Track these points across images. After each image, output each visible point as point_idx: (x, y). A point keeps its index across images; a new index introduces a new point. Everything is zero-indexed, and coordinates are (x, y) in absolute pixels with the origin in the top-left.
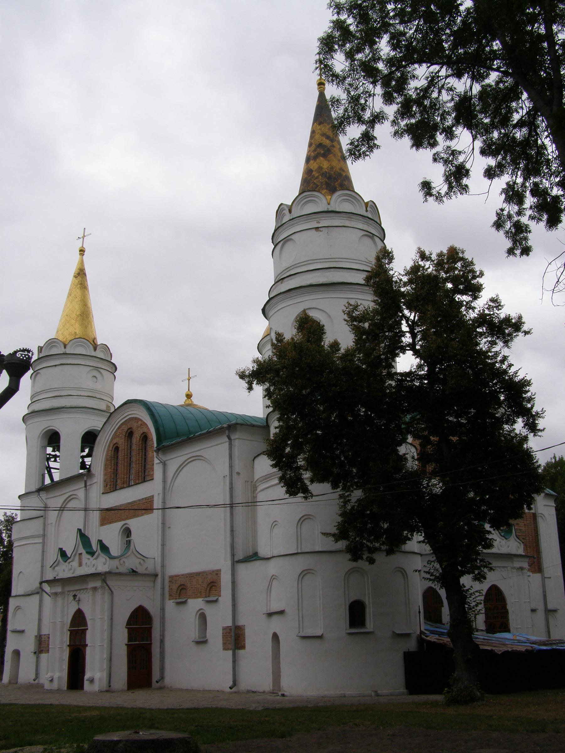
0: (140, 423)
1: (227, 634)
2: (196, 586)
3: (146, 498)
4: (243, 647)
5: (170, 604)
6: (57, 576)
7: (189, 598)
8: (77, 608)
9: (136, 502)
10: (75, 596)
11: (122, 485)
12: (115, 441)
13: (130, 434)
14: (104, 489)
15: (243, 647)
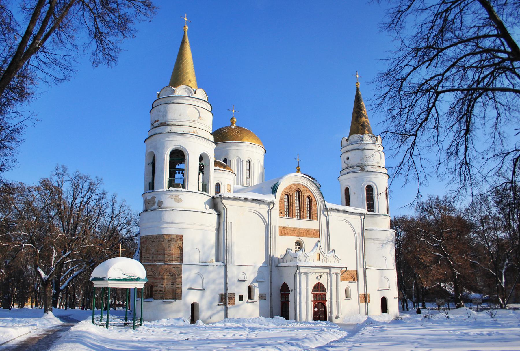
3: (313, 229)
12: (287, 191)
13: (299, 192)
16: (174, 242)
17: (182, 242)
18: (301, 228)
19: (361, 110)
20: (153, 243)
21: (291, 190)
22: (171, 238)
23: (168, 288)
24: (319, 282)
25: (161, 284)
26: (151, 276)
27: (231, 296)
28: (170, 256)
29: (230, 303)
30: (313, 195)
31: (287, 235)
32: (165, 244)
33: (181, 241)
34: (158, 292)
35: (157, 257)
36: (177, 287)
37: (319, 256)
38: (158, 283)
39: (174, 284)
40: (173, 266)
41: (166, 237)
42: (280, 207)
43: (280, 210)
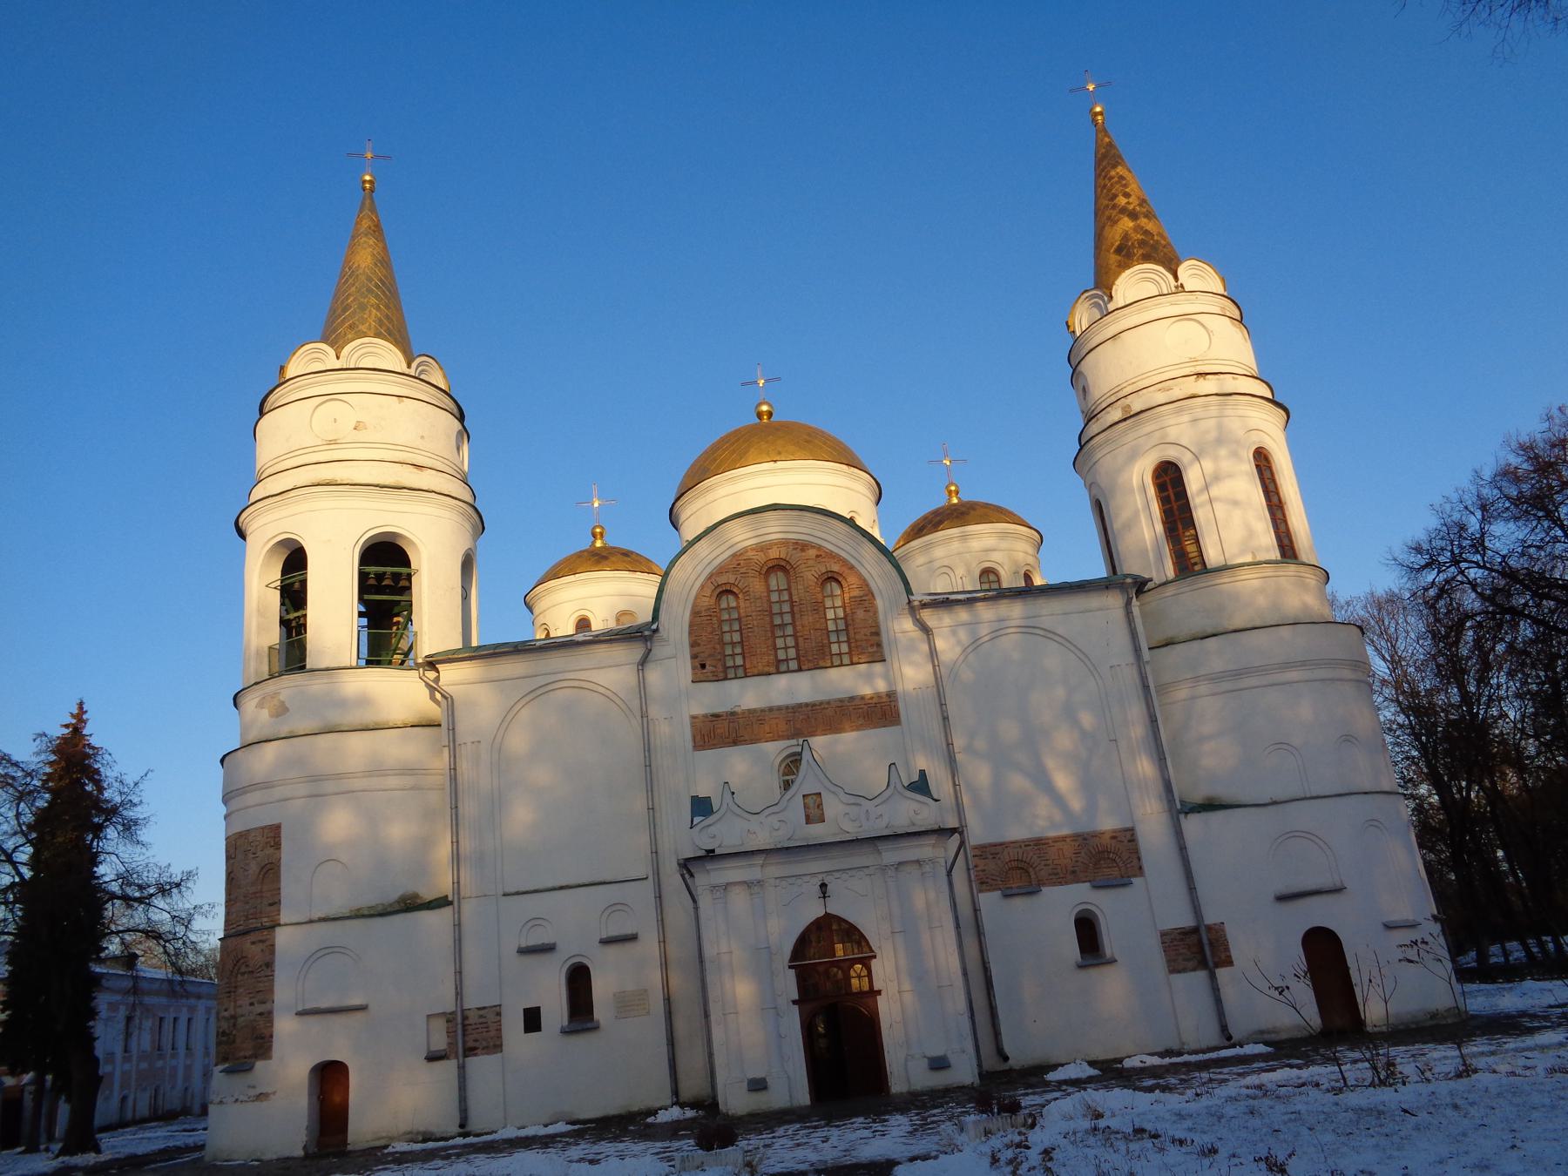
0: (812, 553)
1: (1175, 943)
2: (1055, 862)
4: (1229, 962)
5: (989, 900)
6: (720, 846)
7: (1044, 885)
8: (822, 913)
9: (828, 703)
10: (823, 886)
11: (766, 669)
12: (722, 580)
14: (694, 674)
15: (1229, 962)
16: (259, 854)
18: (800, 706)
19: (1115, 196)
21: (743, 570)
23: (243, 1018)
24: (827, 915)
27: (481, 1016)
28: (247, 903)
29: (477, 1044)
30: (852, 568)
33: (277, 845)
36: (261, 1014)
37: (820, 806)
42: (693, 645)
43: (694, 657)
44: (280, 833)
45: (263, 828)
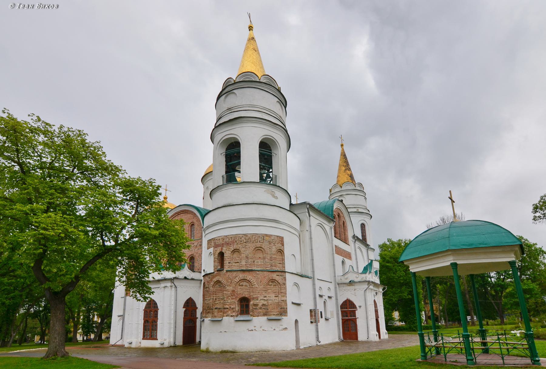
16: (276, 245)
17: (283, 245)
20: (247, 244)
22: (272, 238)
23: (271, 301)
25: (263, 296)
26: (244, 287)
30: (346, 222)
31: (338, 254)
32: (265, 246)
34: (259, 307)
35: (254, 262)
36: (283, 301)
38: (259, 295)
39: (277, 296)
40: (278, 274)
41: (266, 238)
44: (283, 240)
45: (277, 236)
